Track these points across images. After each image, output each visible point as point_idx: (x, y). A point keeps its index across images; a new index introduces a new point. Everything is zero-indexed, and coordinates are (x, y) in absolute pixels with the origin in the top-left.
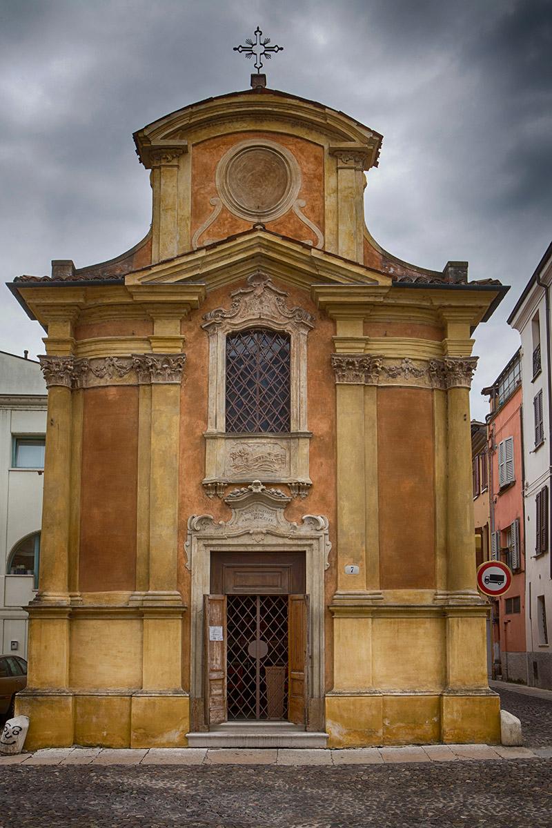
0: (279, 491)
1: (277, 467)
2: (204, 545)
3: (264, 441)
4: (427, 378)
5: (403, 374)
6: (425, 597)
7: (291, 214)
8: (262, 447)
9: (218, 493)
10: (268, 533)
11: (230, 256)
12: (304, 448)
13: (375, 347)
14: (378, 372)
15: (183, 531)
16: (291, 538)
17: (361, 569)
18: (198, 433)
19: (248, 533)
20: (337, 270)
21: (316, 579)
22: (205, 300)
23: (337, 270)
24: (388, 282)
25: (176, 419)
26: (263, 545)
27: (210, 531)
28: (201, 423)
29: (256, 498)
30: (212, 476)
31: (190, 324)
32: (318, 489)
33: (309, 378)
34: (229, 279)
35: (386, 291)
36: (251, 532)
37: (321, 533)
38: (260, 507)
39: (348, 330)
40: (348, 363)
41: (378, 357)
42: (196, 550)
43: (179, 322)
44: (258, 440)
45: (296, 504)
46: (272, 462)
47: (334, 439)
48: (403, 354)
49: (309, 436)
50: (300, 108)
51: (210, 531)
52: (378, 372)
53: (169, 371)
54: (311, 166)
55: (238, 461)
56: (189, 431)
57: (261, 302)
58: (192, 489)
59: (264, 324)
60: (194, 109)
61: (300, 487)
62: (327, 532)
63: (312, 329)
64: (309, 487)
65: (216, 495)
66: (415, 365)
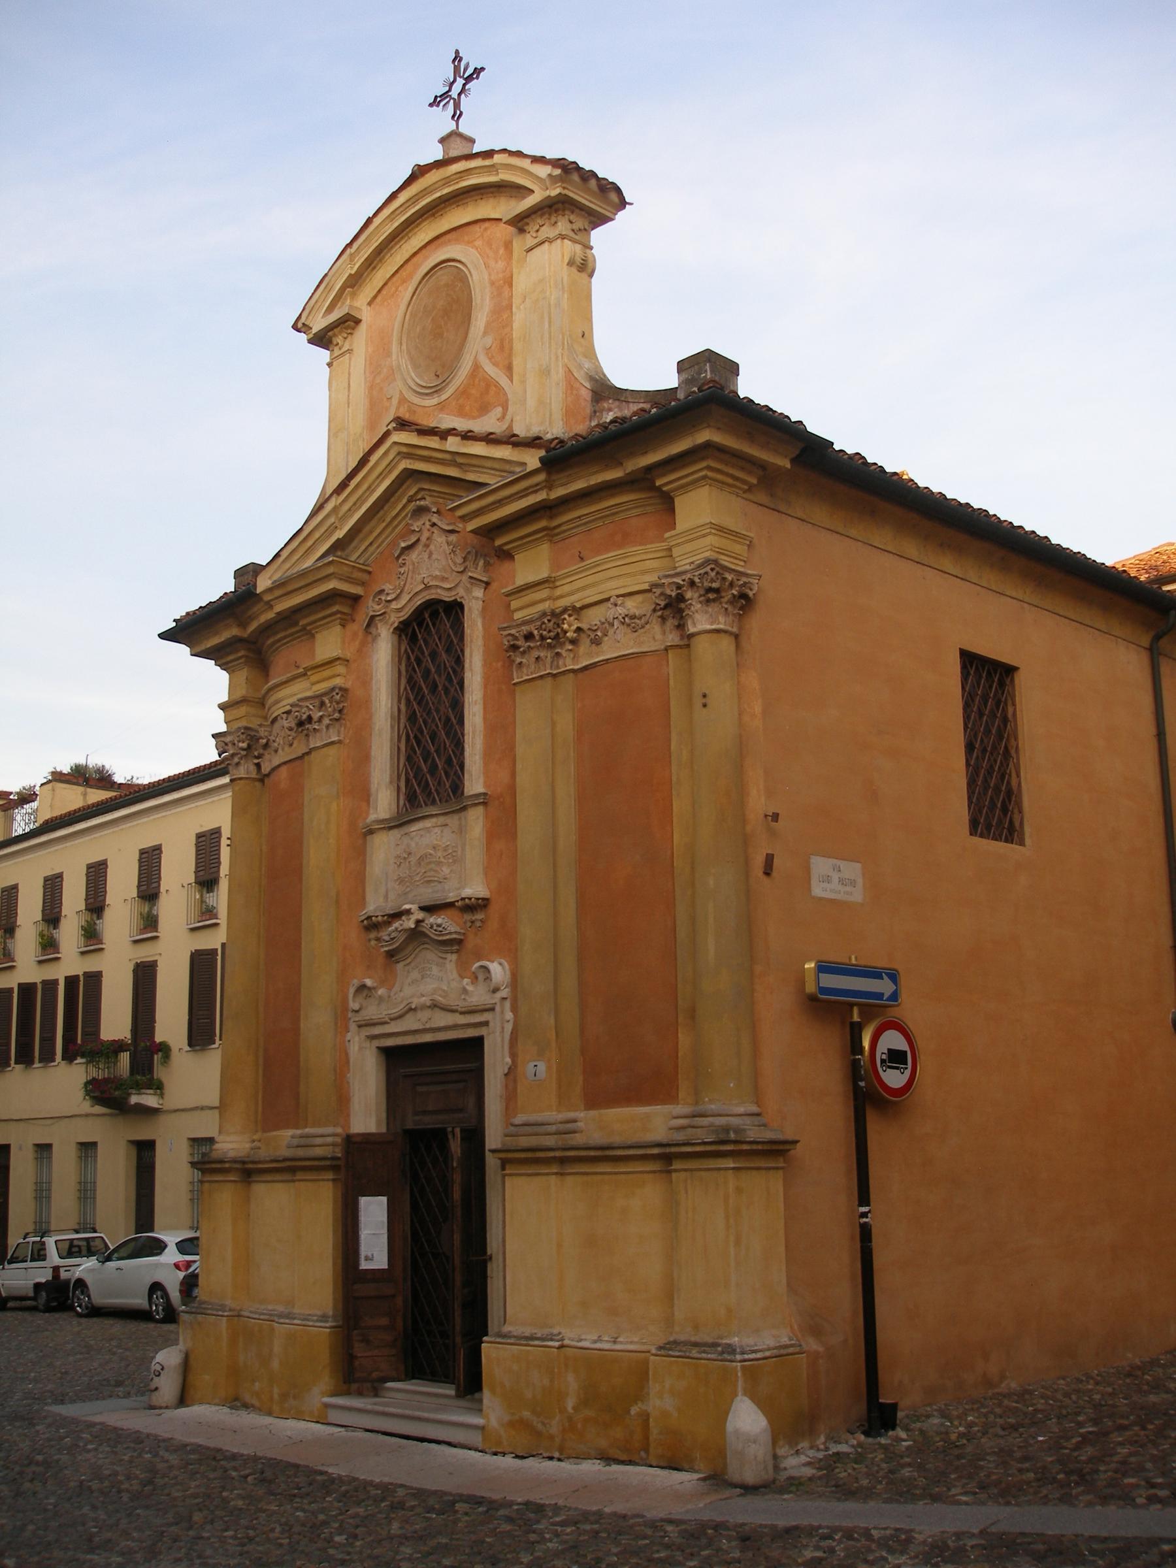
0: (439, 921)
1: (446, 870)
2: (368, 1037)
3: (428, 823)
4: (655, 628)
5: (611, 632)
6: (655, 1121)
7: (476, 367)
8: (431, 833)
10: (435, 1006)
11: (371, 489)
13: (567, 589)
14: (573, 642)
15: (342, 1016)
16: (462, 1013)
17: (549, 1068)
19: (411, 1009)
20: (474, 461)
22: (365, 575)
23: (474, 461)
24: (532, 459)
27: (372, 1011)
30: (375, 904)
32: (494, 910)
34: (389, 530)
35: (541, 477)
39: (530, 566)
40: (529, 637)
41: (565, 610)
42: (356, 1048)
43: (338, 629)
45: (472, 942)
46: (439, 863)
48: (612, 587)
49: (483, 800)
50: (468, 172)
52: (573, 642)
53: (326, 721)
54: (501, 265)
60: (355, 246)
61: (472, 907)
63: (487, 584)
66: (632, 606)
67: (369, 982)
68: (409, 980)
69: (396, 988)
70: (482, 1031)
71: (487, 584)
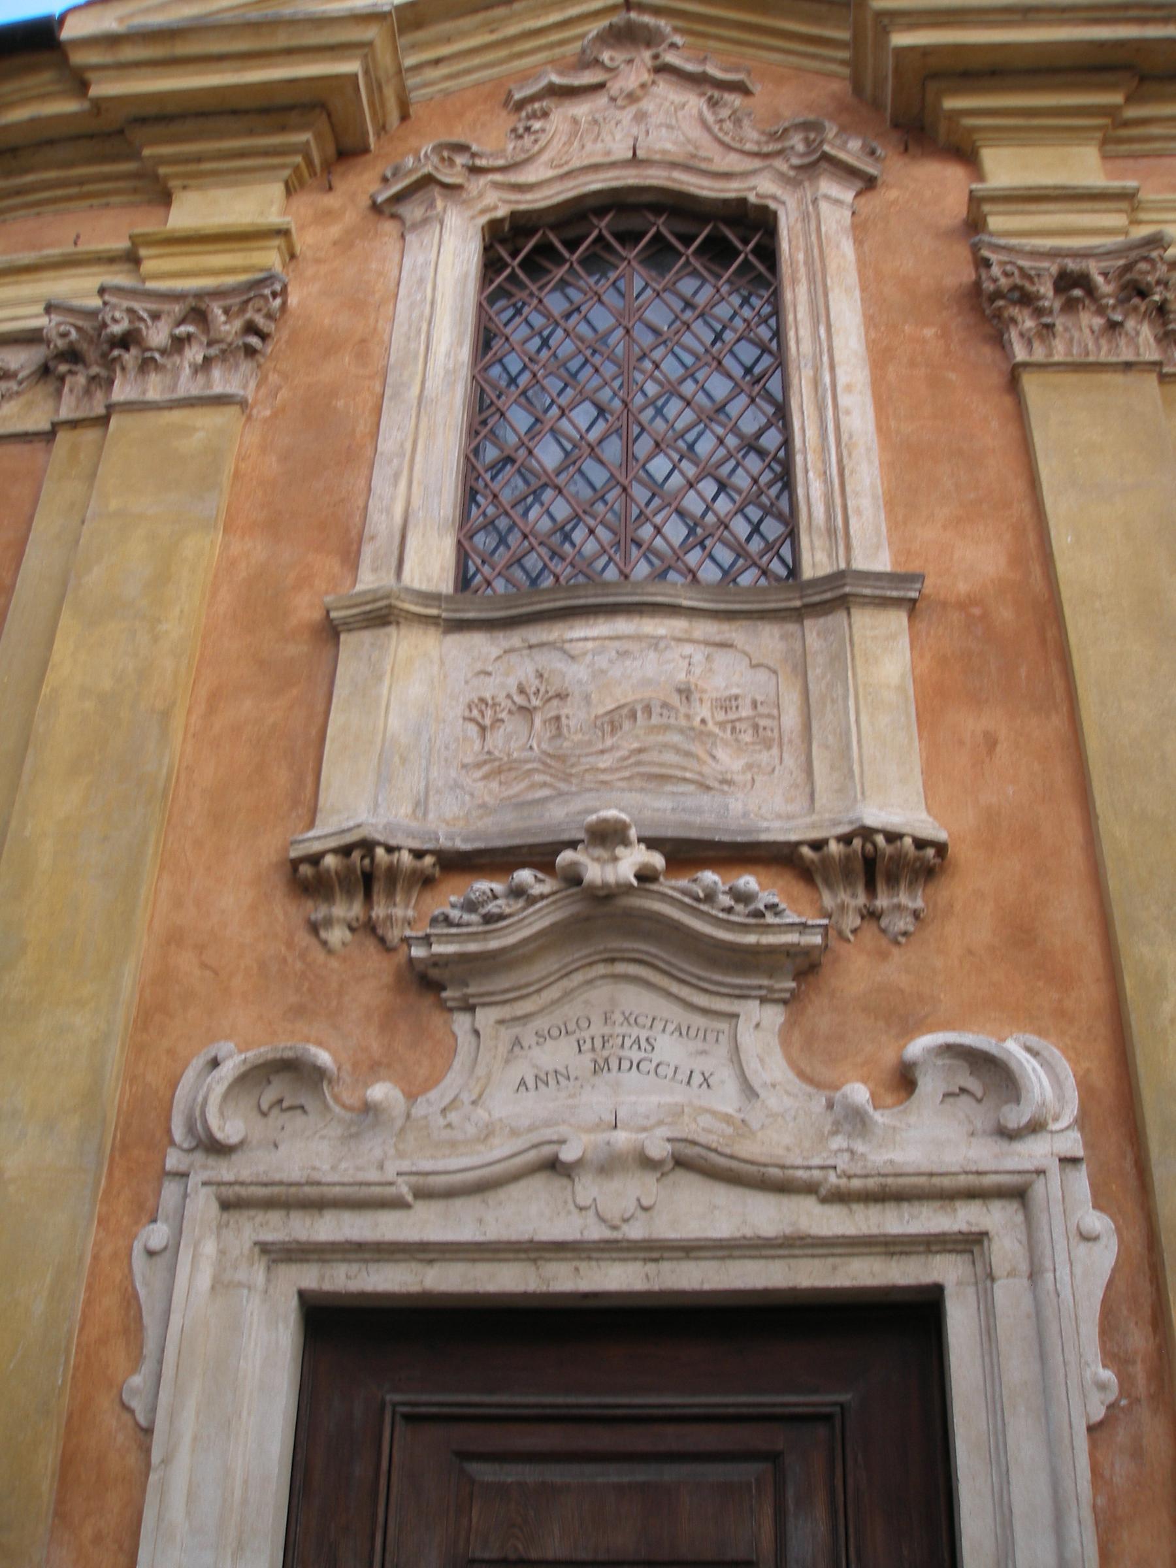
1: (729, 761)
2: (264, 1248)
9: (379, 911)
10: (690, 1163)
12: (885, 653)
16: (840, 1197)
18: (305, 609)
19: (553, 1166)
21: (1029, 1491)
25: (202, 549)
26: (653, 1250)
27: (305, 1151)
28: (332, 565)
29: (605, 924)
31: (330, 201)
33: (880, 357)
34: (503, 53)
36: (568, 1154)
37: (1036, 1152)
38: (634, 999)
42: (204, 1281)
43: (278, 189)
44: (623, 625)
45: (858, 971)
46: (701, 734)
47: (1049, 613)
49: (901, 593)
51: (305, 1151)
55: (510, 738)
56: (259, 602)
57: (641, 117)
58: (239, 905)
59: (655, 177)
61: (877, 864)
62: (1072, 1143)
64: (924, 863)
65: (369, 928)
67: (324, 1058)
68: (522, 1069)
69: (453, 1082)
70: (945, 1271)
71: (869, 183)
